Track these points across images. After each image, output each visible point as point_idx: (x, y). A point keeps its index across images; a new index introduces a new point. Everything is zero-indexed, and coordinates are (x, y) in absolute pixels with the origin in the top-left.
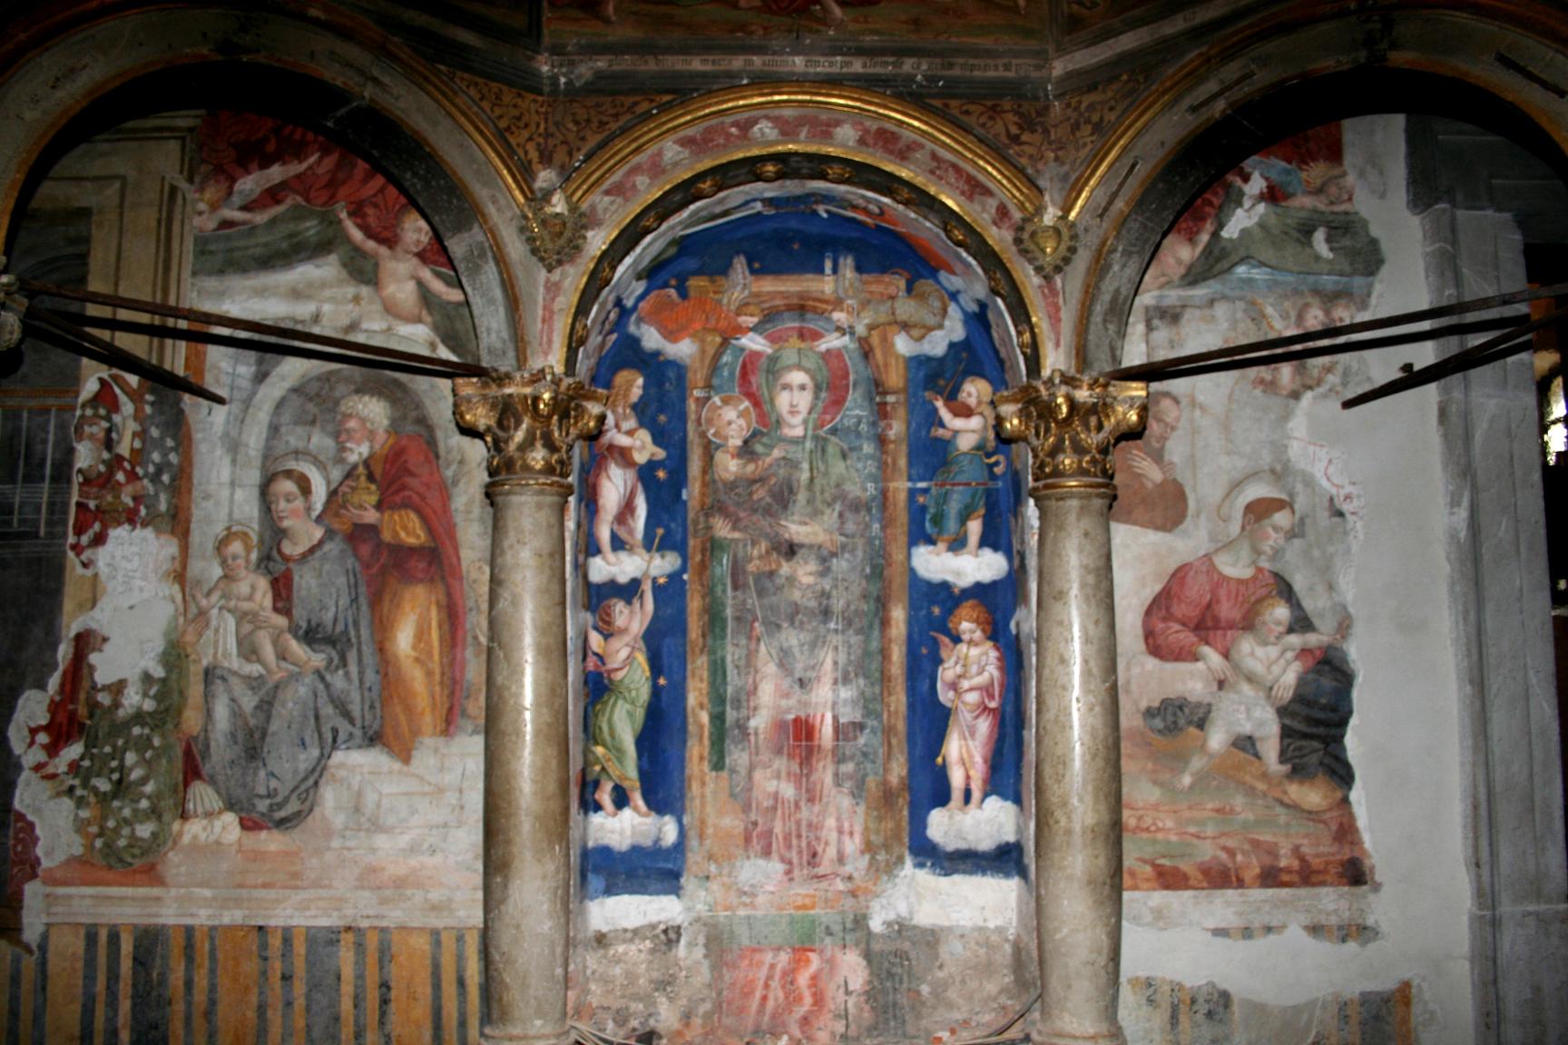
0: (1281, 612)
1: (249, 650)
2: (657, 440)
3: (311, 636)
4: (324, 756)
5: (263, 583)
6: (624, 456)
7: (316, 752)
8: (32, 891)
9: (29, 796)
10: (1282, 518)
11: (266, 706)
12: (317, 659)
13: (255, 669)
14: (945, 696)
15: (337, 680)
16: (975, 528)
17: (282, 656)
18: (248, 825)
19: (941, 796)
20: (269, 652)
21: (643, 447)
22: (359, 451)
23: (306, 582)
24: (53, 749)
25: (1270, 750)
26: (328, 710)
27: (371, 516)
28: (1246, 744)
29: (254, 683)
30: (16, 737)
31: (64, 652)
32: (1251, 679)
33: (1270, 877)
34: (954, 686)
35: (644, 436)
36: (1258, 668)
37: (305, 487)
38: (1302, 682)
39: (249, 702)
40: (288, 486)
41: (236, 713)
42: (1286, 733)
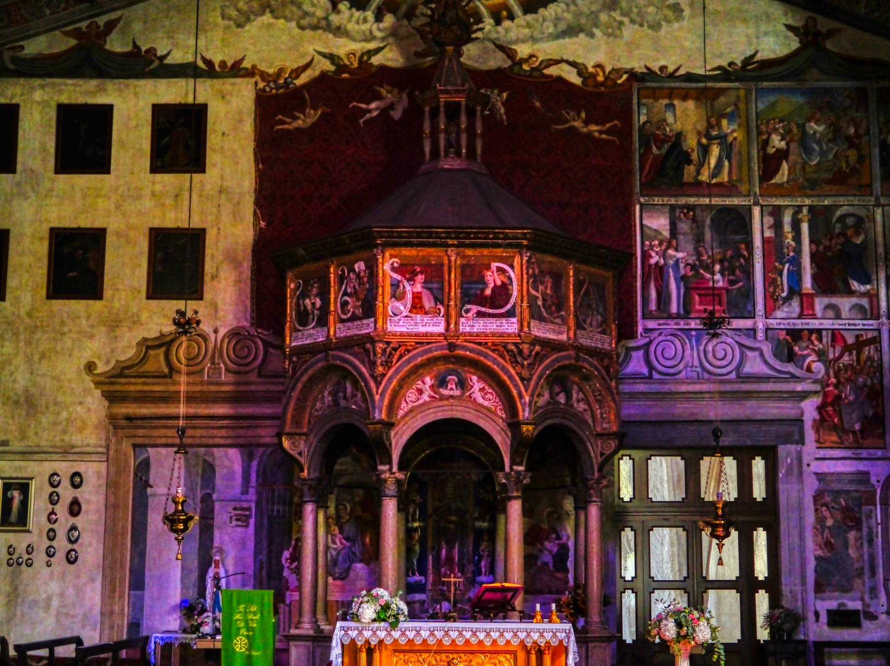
0: (554, 536)
1: (334, 542)
2: (421, 498)
3: (347, 539)
4: (351, 565)
5: (336, 528)
6: (414, 501)
7: (348, 564)
8: (288, 593)
9: (286, 573)
10: (555, 516)
11: (338, 554)
12: (349, 544)
13: (335, 546)
14: (482, 553)
15: (353, 549)
16: (488, 517)
17: (341, 543)
18: (334, 579)
19: (480, 574)
20: (338, 543)
21: (418, 499)
22: (357, 499)
23: (346, 528)
24: (291, 563)
25: (551, 566)
26: (351, 555)
27: (360, 514)
28: (546, 564)
29: (335, 549)
30: (284, 561)
31: (293, 543)
32: (547, 550)
33: (550, 592)
34: (483, 551)
35: (418, 497)
36: (548, 547)
37: (345, 508)
38: (558, 550)
39: (334, 553)
40: (342, 507)
41: (332, 556)
42: (554, 562)
